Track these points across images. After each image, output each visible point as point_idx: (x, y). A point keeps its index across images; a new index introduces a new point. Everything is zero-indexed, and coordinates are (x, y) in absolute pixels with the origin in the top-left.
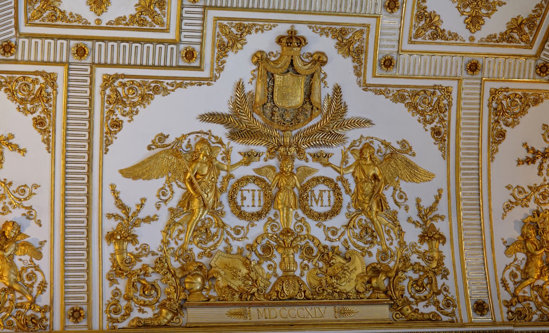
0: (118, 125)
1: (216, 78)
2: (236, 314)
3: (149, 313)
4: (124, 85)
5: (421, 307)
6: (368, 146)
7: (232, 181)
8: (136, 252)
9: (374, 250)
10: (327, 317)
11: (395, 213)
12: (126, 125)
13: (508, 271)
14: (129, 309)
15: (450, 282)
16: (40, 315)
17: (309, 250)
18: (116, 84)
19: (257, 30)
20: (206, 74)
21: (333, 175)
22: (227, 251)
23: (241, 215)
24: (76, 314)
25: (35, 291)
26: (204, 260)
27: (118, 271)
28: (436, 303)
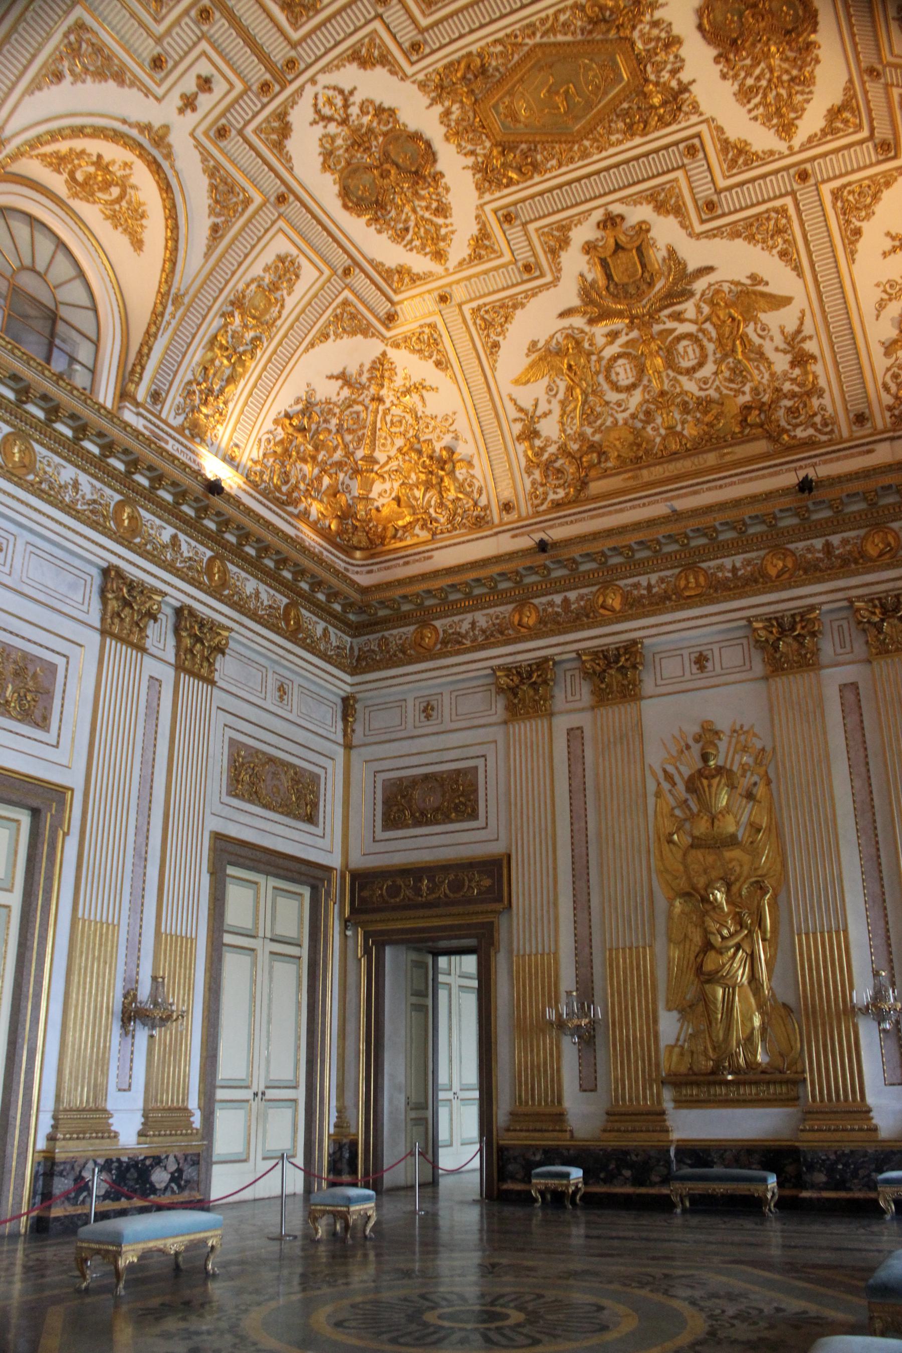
0: (496, 345)
1: (557, 279)
2: (629, 478)
3: (561, 493)
4: (487, 312)
5: (800, 433)
6: (717, 292)
7: (604, 363)
8: (542, 445)
9: (747, 389)
10: (709, 464)
11: (761, 346)
12: (502, 343)
13: (890, 373)
14: (546, 494)
15: (826, 401)
16: (483, 514)
17: (685, 403)
18: (482, 312)
19: (576, 225)
20: (549, 278)
22: (615, 423)
24: (507, 507)
25: (476, 496)
26: (597, 437)
28: (814, 425)
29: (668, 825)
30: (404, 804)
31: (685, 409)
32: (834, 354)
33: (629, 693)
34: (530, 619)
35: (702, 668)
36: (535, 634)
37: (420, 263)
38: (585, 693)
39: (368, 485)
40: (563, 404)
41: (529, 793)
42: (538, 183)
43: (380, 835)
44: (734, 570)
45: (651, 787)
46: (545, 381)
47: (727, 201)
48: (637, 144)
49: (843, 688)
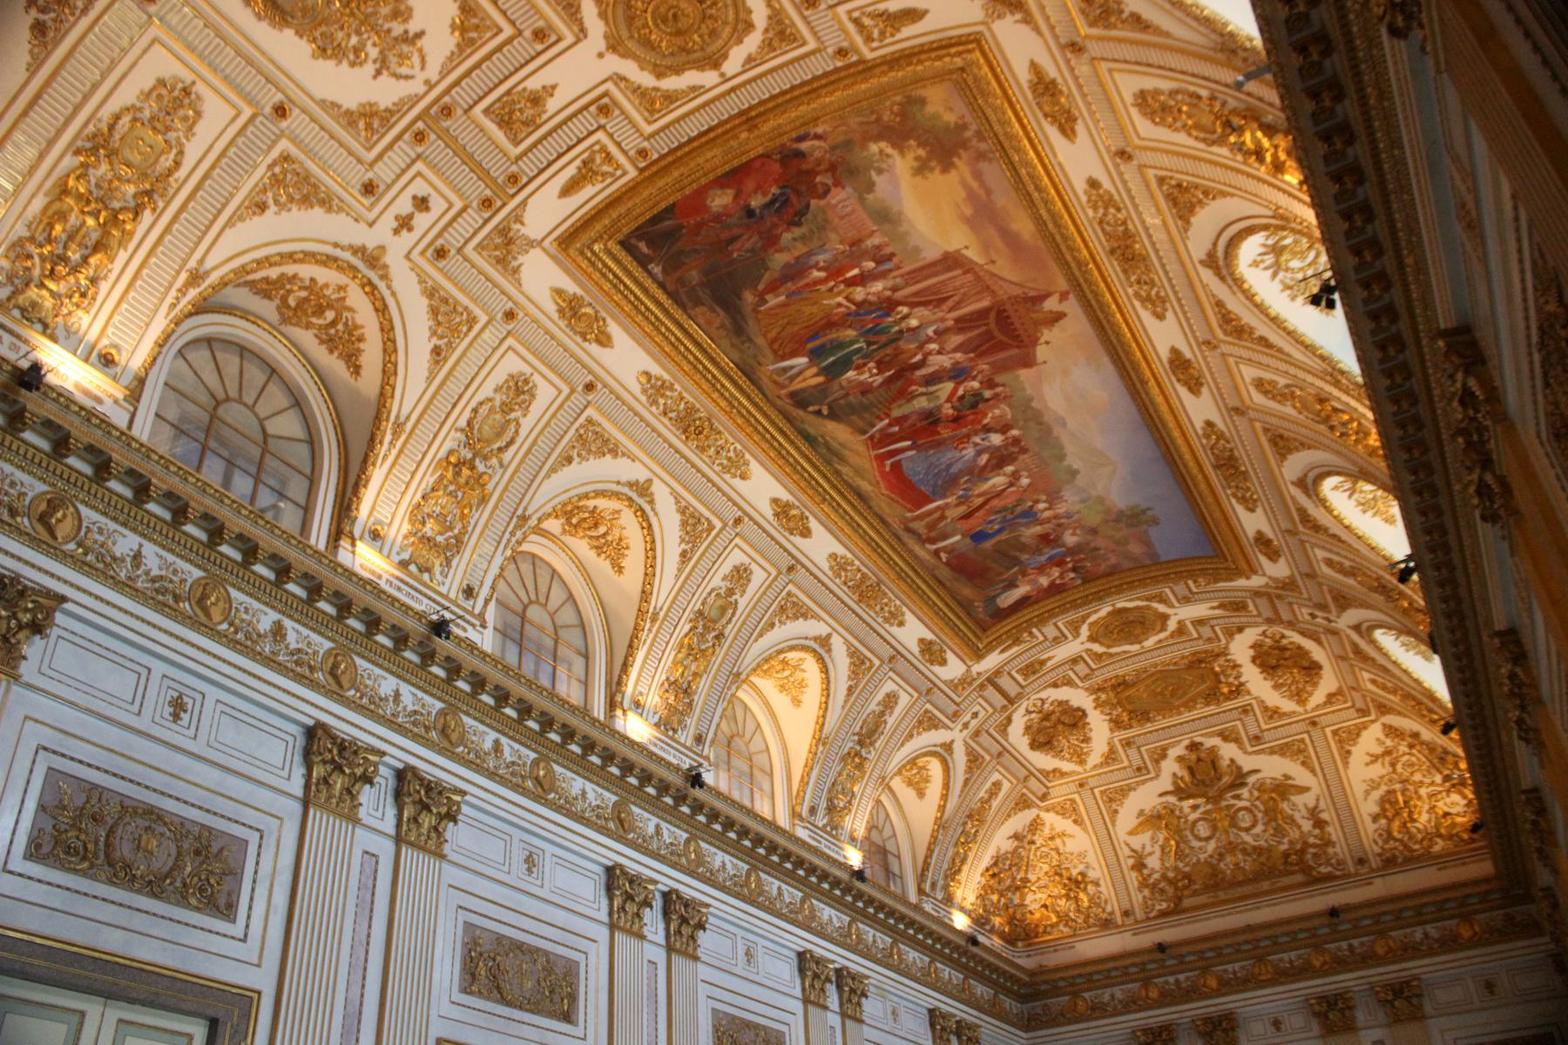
0: (1116, 812)
3: (1164, 905)
5: (1323, 870)
6: (1262, 784)
15: (1338, 849)
21: (1246, 804)
23: (1200, 839)
24: (1126, 914)
26: (1187, 869)
27: (1144, 884)
31: (1244, 851)
34: (1154, 994)
35: (1278, 1029)
36: (1159, 1004)
37: (1066, 766)
39: (1023, 897)
40: (1163, 848)
42: (1149, 727)
44: (1291, 962)
46: (1149, 834)
48: (1212, 709)
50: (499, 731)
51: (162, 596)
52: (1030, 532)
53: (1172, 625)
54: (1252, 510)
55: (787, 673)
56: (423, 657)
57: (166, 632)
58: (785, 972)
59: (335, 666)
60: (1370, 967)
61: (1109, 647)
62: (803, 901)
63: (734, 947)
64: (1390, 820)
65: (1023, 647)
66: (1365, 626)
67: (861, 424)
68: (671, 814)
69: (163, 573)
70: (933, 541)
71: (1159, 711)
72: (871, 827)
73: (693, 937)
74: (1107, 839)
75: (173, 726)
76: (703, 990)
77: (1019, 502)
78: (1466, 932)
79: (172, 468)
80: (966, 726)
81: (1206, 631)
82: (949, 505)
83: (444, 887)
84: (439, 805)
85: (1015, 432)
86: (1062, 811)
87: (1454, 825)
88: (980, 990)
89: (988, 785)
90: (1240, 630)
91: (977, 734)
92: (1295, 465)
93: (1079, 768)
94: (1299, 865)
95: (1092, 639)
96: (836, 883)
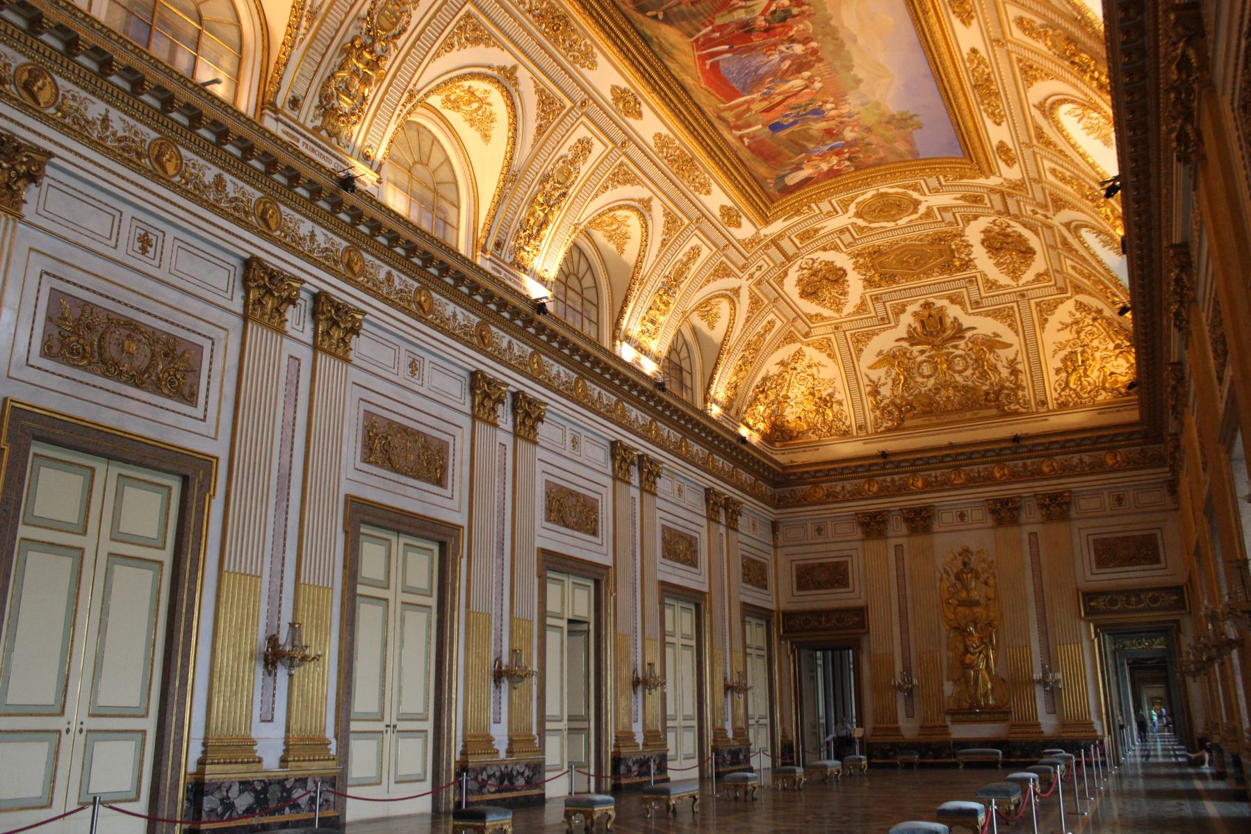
0: (861, 350)
3: (890, 424)
5: (1013, 407)
15: (1026, 393)
24: (860, 428)
27: (877, 406)
29: (946, 595)
30: (808, 577)
31: (955, 388)
32: (1031, 372)
33: (927, 530)
34: (875, 489)
35: (962, 520)
37: (826, 313)
38: (904, 529)
40: (894, 381)
41: (874, 575)
42: (894, 287)
43: (796, 593)
45: (938, 576)
47: (985, 302)
48: (945, 277)
49: (1030, 534)
50: (390, 265)
51: (127, 153)
52: (817, 127)
53: (922, 209)
54: (999, 124)
55: (614, 227)
56: (333, 205)
57: (132, 182)
58: (599, 456)
59: (265, 212)
60: (1035, 480)
61: (870, 222)
62: (617, 404)
63: (564, 435)
64: (1069, 375)
65: (802, 217)
66: (1073, 224)
67: (689, 28)
68: (520, 334)
69: (127, 134)
70: (739, 128)
71: (903, 276)
72: (672, 349)
73: (533, 428)
74: (851, 372)
75: (141, 257)
76: (540, 466)
77: (812, 101)
78: (1110, 461)
79: (129, 47)
80: (751, 276)
81: (948, 217)
82: (755, 100)
83: (349, 384)
84: (346, 322)
85: (814, 44)
86: (820, 348)
87: (1116, 382)
88: (745, 476)
89: (765, 323)
90: (976, 218)
91: (759, 283)
92: (1040, 90)
93: (836, 315)
94: (997, 401)
95: (858, 215)
96: (643, 391)
